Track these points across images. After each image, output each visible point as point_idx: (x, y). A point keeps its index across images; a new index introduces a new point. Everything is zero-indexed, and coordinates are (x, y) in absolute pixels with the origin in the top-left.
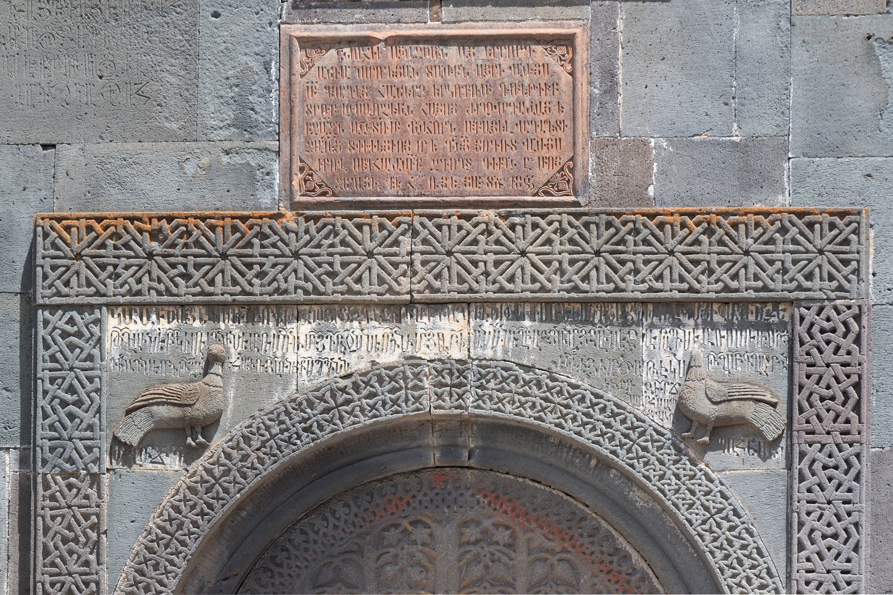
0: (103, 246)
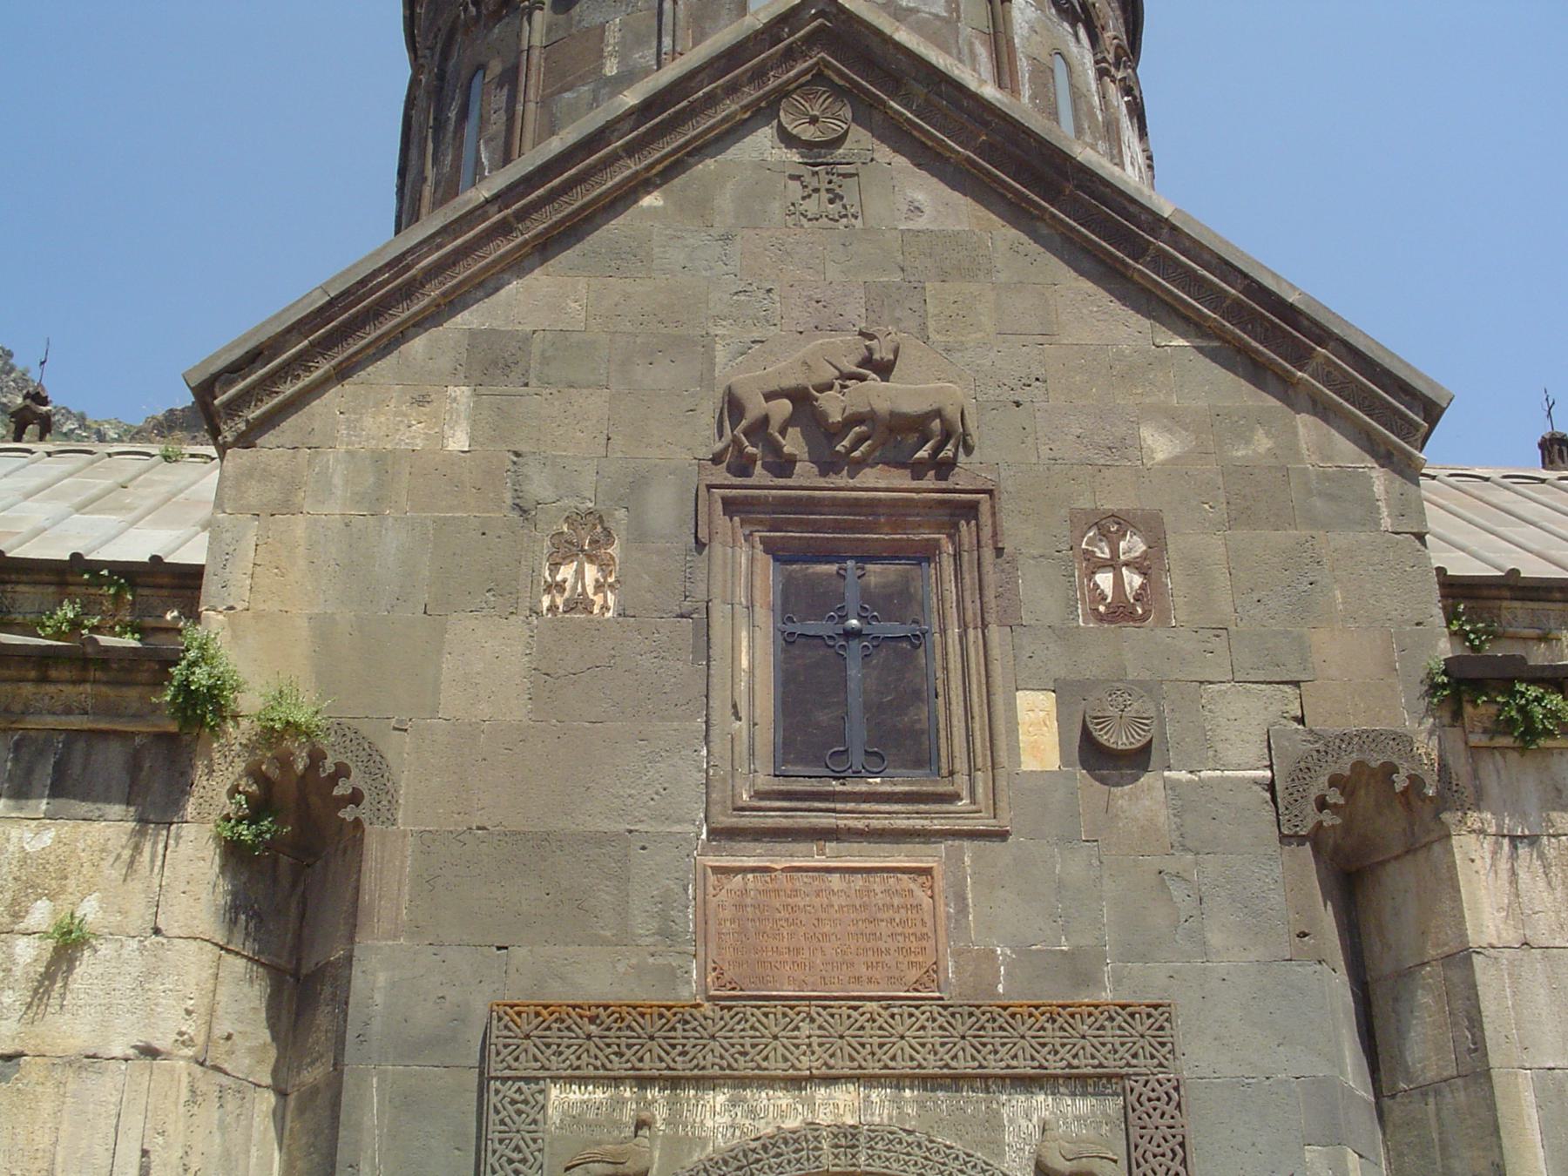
0: (549, 1028)
